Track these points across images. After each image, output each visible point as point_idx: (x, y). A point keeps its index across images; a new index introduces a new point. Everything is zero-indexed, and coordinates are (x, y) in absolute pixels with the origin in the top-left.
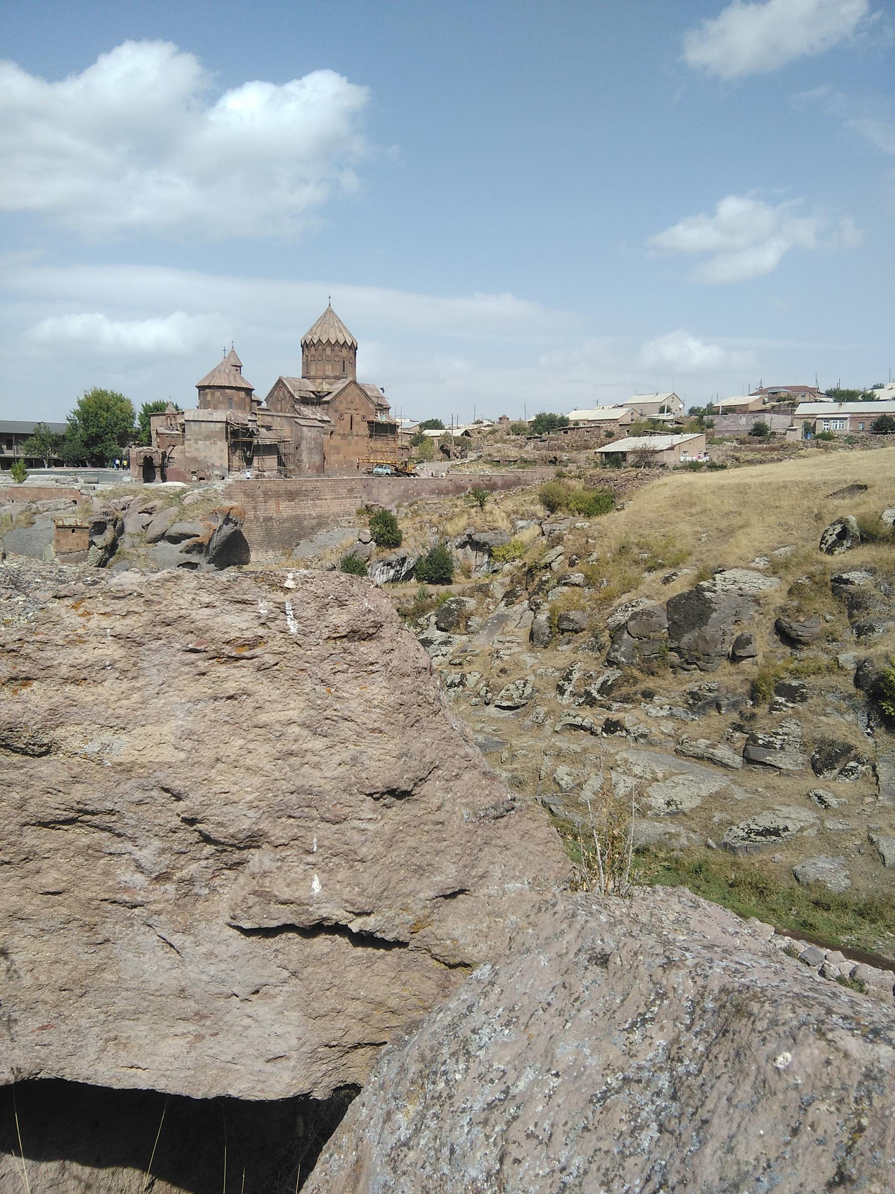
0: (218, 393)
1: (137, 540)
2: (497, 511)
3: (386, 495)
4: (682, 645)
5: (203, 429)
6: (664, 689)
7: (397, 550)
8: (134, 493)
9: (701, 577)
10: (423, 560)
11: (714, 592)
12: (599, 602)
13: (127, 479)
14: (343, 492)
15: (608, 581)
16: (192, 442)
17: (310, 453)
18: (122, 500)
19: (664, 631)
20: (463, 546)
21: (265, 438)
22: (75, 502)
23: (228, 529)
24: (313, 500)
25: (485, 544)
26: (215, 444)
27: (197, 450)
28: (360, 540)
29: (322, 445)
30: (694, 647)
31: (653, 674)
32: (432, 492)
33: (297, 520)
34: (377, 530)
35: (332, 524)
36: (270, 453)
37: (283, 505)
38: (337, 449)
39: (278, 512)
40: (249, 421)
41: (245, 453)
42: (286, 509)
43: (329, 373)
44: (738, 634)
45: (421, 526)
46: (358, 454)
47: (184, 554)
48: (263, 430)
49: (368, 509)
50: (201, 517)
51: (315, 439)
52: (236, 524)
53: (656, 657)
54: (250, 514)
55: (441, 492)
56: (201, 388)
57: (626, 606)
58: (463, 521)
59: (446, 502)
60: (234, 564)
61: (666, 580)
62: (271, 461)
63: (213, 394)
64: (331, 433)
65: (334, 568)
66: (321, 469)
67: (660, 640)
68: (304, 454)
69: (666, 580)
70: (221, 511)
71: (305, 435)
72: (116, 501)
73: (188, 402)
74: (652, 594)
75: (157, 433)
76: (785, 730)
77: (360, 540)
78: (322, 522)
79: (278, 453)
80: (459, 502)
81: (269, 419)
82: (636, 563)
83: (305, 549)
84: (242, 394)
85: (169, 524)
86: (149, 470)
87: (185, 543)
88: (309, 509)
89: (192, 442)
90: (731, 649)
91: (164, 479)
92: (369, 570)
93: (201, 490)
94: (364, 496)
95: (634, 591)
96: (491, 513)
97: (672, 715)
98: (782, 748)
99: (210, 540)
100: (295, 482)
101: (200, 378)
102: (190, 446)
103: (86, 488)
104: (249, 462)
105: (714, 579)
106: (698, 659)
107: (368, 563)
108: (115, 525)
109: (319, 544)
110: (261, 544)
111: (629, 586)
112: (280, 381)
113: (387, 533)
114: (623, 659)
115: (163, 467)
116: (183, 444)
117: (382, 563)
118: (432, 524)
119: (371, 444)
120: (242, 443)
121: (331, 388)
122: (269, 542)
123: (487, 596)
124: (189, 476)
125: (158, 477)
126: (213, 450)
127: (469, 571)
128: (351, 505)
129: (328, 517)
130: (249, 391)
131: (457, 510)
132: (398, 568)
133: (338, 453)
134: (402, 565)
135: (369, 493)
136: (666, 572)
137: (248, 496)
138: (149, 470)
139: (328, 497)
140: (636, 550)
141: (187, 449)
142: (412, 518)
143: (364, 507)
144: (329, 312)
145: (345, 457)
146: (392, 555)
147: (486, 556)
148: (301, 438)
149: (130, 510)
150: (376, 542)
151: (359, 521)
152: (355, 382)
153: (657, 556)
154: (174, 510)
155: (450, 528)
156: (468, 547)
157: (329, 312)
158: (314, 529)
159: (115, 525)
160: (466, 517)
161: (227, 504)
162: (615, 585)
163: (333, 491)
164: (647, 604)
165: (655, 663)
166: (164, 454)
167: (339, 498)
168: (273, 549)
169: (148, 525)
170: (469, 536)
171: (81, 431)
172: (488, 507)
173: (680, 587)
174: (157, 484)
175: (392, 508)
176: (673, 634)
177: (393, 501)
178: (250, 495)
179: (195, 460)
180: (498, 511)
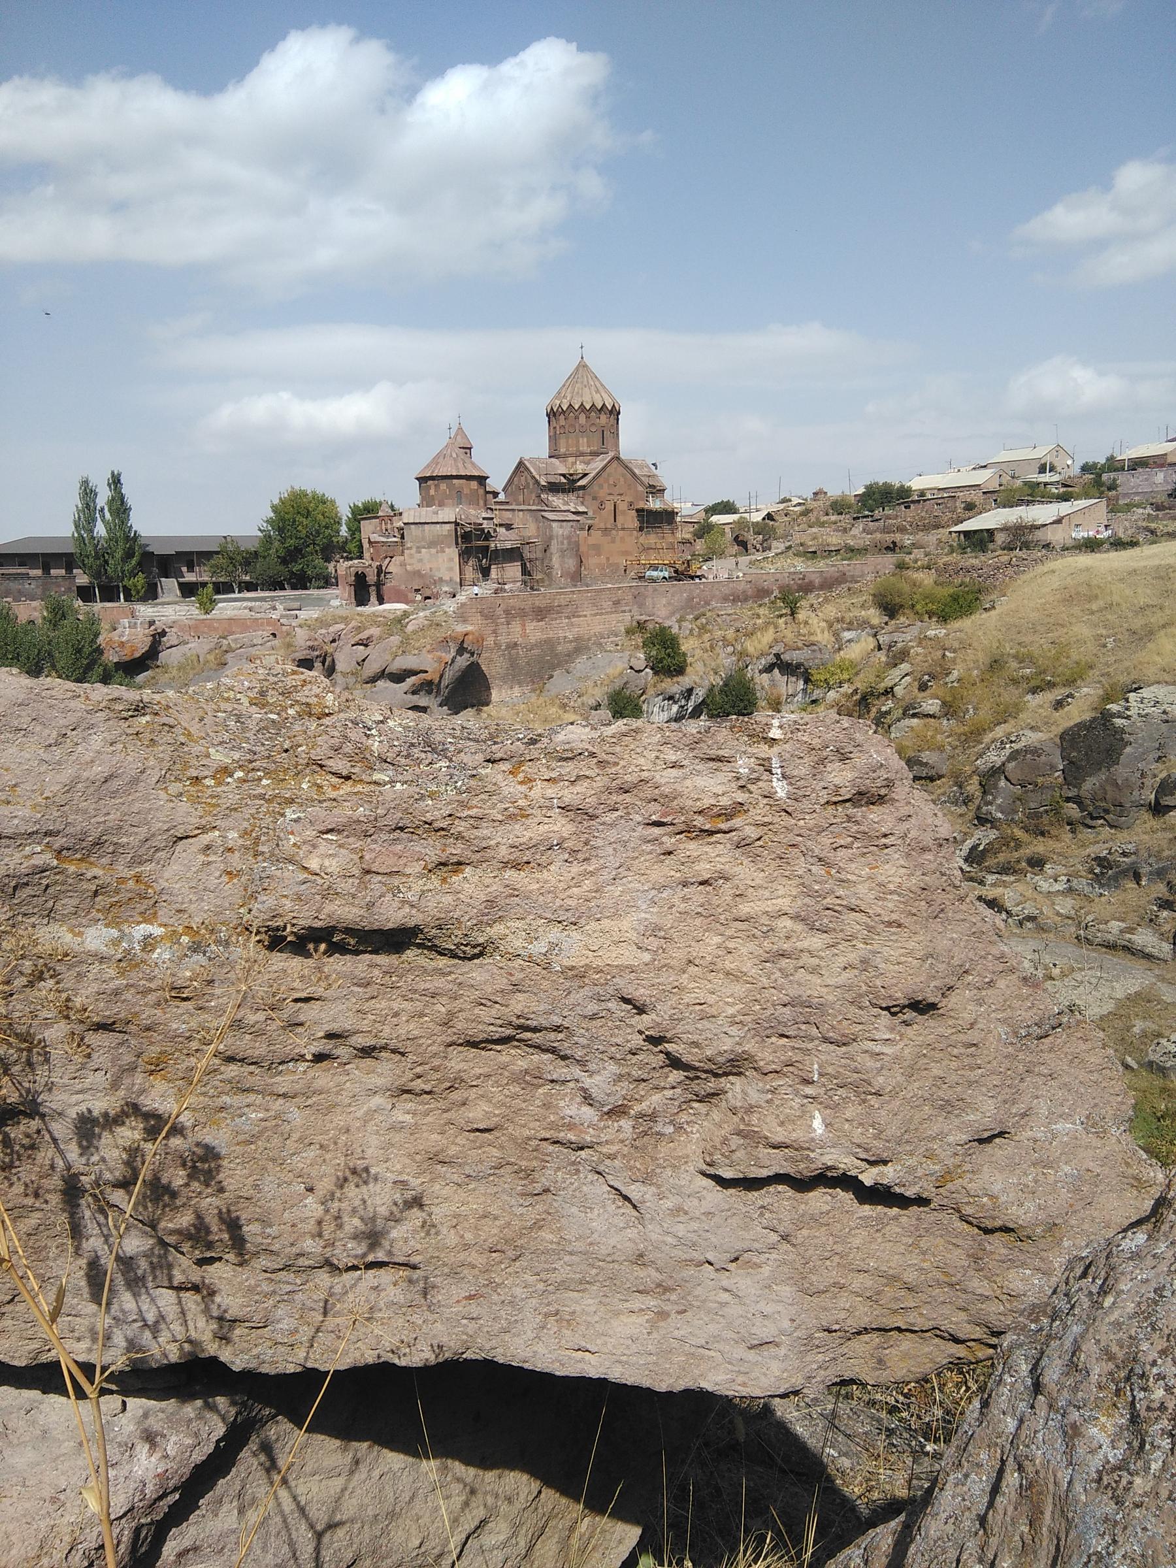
0: (443, 486)
2: (814, 621)
3: (664, 607)
4: (1083, 793)
6: (1059, 854)
7: (680, 679)
8: (345, 620)
9: (1108, 698)
10: (716, 690)
11: (1128, 717)
12: (963, 738)
13: (335, 603)
15: (975, 709)
16: (413, 551)
17: (562, 556)
18: (331, 629)
19: (1057, 774)
20: (769, 669)
21: (504, 540)
22: (274, 635)
23: (463, 661)
25: (799, 666)
27: (420, 561)
28: (631, 668)
29: (577, 544)
30: (1100, 795)
32: (725, 599)
34: (654, 653)
35: (594, 648)
36: (512, 560)
37: (531, 626)
38: (597, 548)
39: (524, 635)
42: (534, 632)
43: (584, 448)
44: (1163, 775)
45: (712, 647)
46: (626, 553)
47: (410, 696)
48: (502, 530)
49: (641, 626)
50: (428, 647)
51: (569, 538)
52: (472, 654)
53: (1046, 811)
54: (490, 641)
55: (737, 598)
56: (422, 480)
57: (1002, 742)
58: (768, 636)
59: (744, 612)
60: (472, 706)
61: (1059, 705)
62: (513, 570)
64: (589, 528)
65: (597, 707)
66: (577, 577)
67: (1052, 788)
69: (1059, 705)
70: (454, 639)
72: (323, 631)
73: (406, 498)
74: (1039, 724)
75: (370, 542)
77: (631, 668)
78: (580, 647)
79: (522, 559)
80: (762, 611)
81: (509, 515)
82: (1015, 682)
83: (560, 683)
85: (390, 658)
86: (362, 590)
88: (563, 630)
89: (413, 551)
90: (1153, 796)
91: (381, 601)
92: (645, 707)
93: (427, 613)
94: (635, 608)
95: (1012, 722)
96: (806, 623)
99: (441, 676)
100: (545, 595)
101: (420, 467)
102: (411, 556)
103: (286, 616)
104: (485, 572)
105: (1127, 700)
106: (1107, 811)
107: (642, 698)
108: (323, 663)
109: (578, 675)
110: (504, 679)
111: (1004, 715)
112: (521, 464)
113: (666, 658)
114: (999, 815)
115: (379, 585)
116: (402, 554)
117: (661, 697)
118: (726, 642)
119: (641, 540)
120: (476, 547)
121: (587, 469)
122: (514, 675)
124: (411, 595)
125: (373, 598)
126: (440, 560)
127: (779, 703)
129: (589, 639)
130: (482, 480)
131: (759, 621)
132: (683, 702)
134: (688, 698)
135: (641, 605)
136: (1058, 693)
137: (486, 617)
138: (362, 590)
139: (588, 613)
140: (1014, 664)
141: (408, 561)
142: (700, 636)
143: (635, 624)
144: (582, 366)
145: (608, 559)
146: (674, 686)
147: (802, 682)
148: (551, 538)
150: (652, 669)
151: (629, 643)
152: (617, 458)
153: (1044, 672)
154: (395, 640)
155: (751, 646)
156: (776, 671)
157: (582, 366)
158: (571, 656)
159: (323, 663)
160: (771, 630)
161: (461, 628)
162: (985, 714)
164: (1031, 738)
165: (1045, 819)
166: (379, 568)
167: (602, 614)
168: (520, 684)
170: (777, 656)
172: (801, 616)
173: (1078, 712)
174: (373, 608)
175: (672, 624)
176: (1069, 779)
177: (673, 614)
178: (488, 616)
179: (417, 574)
180: (815, 620)
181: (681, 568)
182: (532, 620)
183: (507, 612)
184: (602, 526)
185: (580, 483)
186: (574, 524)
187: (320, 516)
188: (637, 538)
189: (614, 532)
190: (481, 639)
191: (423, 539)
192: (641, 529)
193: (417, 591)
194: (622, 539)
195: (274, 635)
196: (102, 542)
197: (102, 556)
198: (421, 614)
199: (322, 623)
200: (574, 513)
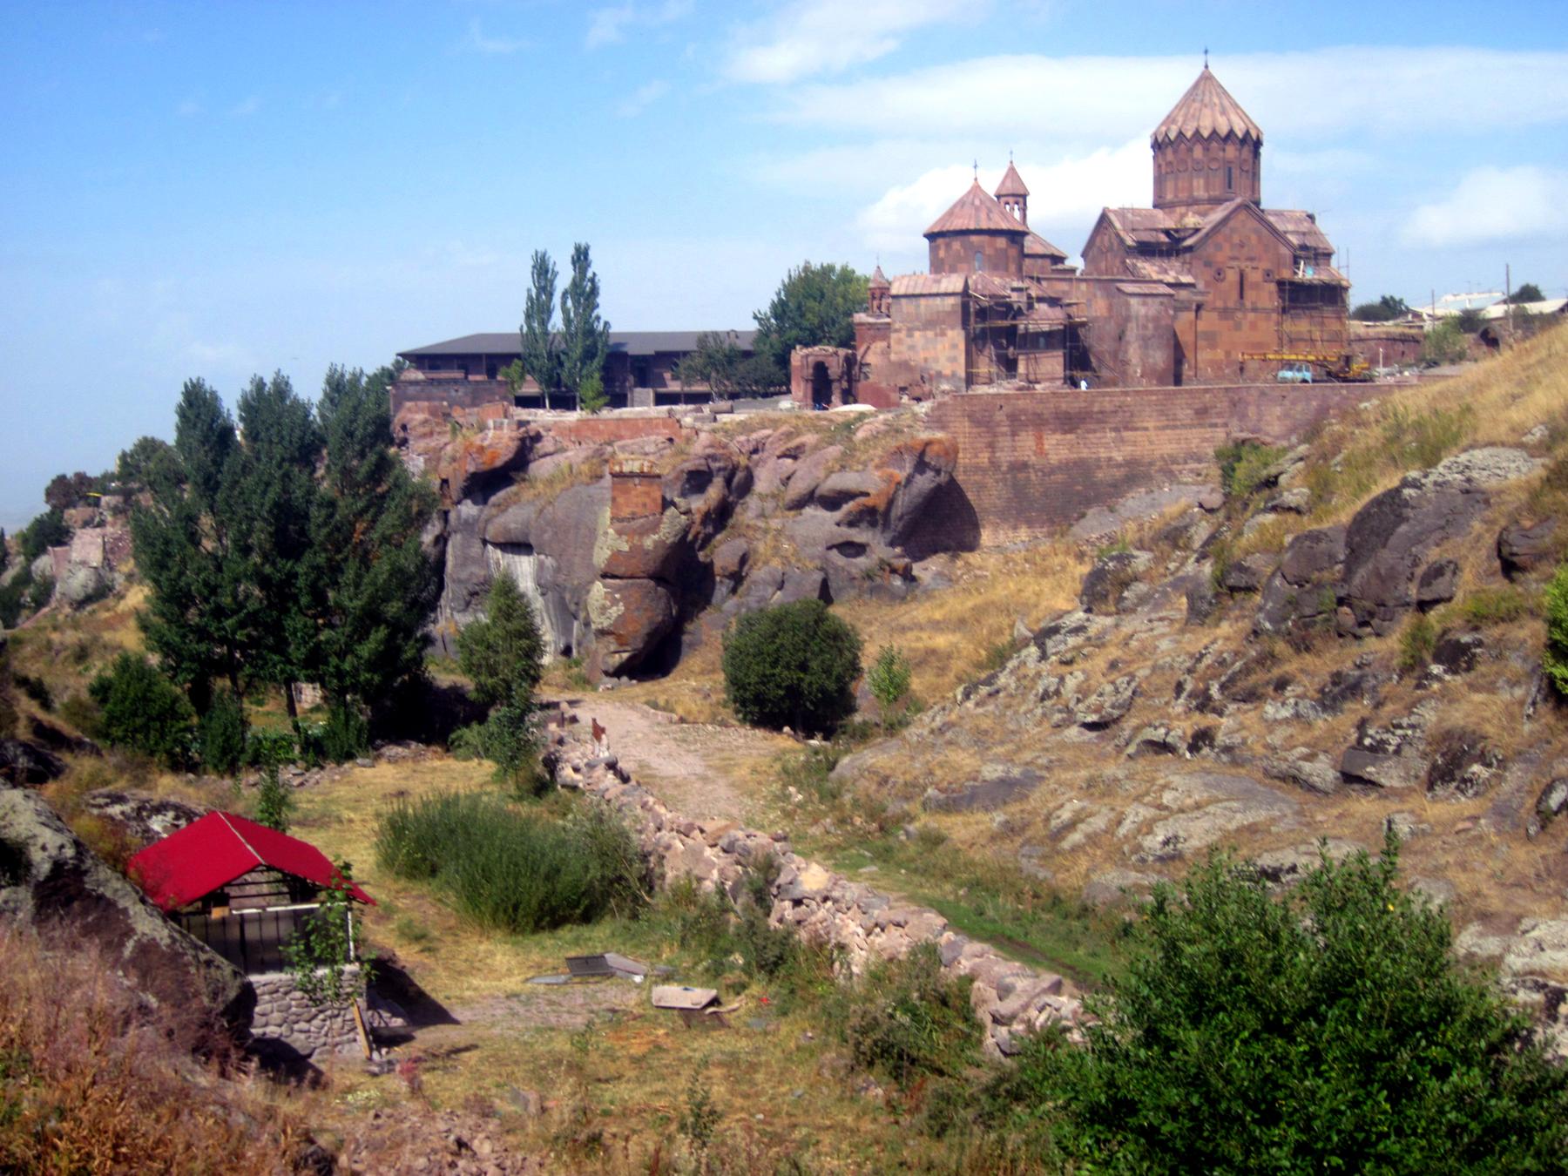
0: (956, 245)
1: (770, 505)
4: (1355, 592)
5: (922, 309)
14: (1185, 414)
18: (754, 436)
23: (924, 482)
24: (1116, 430)
26: (943, 334)
27: (912, 348)
31: (1308, 649)
33: (1082, 468)
36: (1050, 346)
38: (1212, 339)
39: (1041, 452)
40: (1013, 290)
41: (998, 346)
42: (1058, 448)
48: (1042, 307)
50: (877, 461)
51: (1156, 319)
56: (931, 237)
63: (948, 246)
68: (1131, 351)
71: (1133, 312)
72: (742, 438)
76: (1414, 720)
81: (1064, 286)
84: (1001, 242)
85: (822, 474)
87: (848, 507)
93: (890, 416)
97: (1297, 715)
98: (1398, 752)
102: (900, 341)
104: (1010, 366)
112: (1104, 220)
114: (1268, 625)
120: (994, 330)
123: (1176, 546)
124: (894, 396)
126: (939, 347)
128: (1204, 440)
130: (1016, 236)
133: (1213, 346)
135: (1243, 417)
138: (821, 390)
139: (1150, 425)
145: (1228, 354)
148: (1127, 319)
149: (766, 454)
154: (834, 451)
163: (1162, 413)
167: (1175, 427)
169: (789, 478)
171: (774, 336)
174: (841, 410)
179: (905, 366)
181: (1333, 369)
182: (1054, 431)
183: (1013, 418)
184: (1219, 304)
185: (1189, 242)
186: (1165, 300)
187: (840, 300)
188: (1279, 324)
189: (1239, 315)
190: (951, 452)
191: (918, 317)
192: (1284, 311)
193: (903, 389)
194: (1253, 326)
195: (671, 440)
196: (559, 338)
197: (557, 359)
198: (881, 417)
199: (745, 427)
200: (1170, 285)
